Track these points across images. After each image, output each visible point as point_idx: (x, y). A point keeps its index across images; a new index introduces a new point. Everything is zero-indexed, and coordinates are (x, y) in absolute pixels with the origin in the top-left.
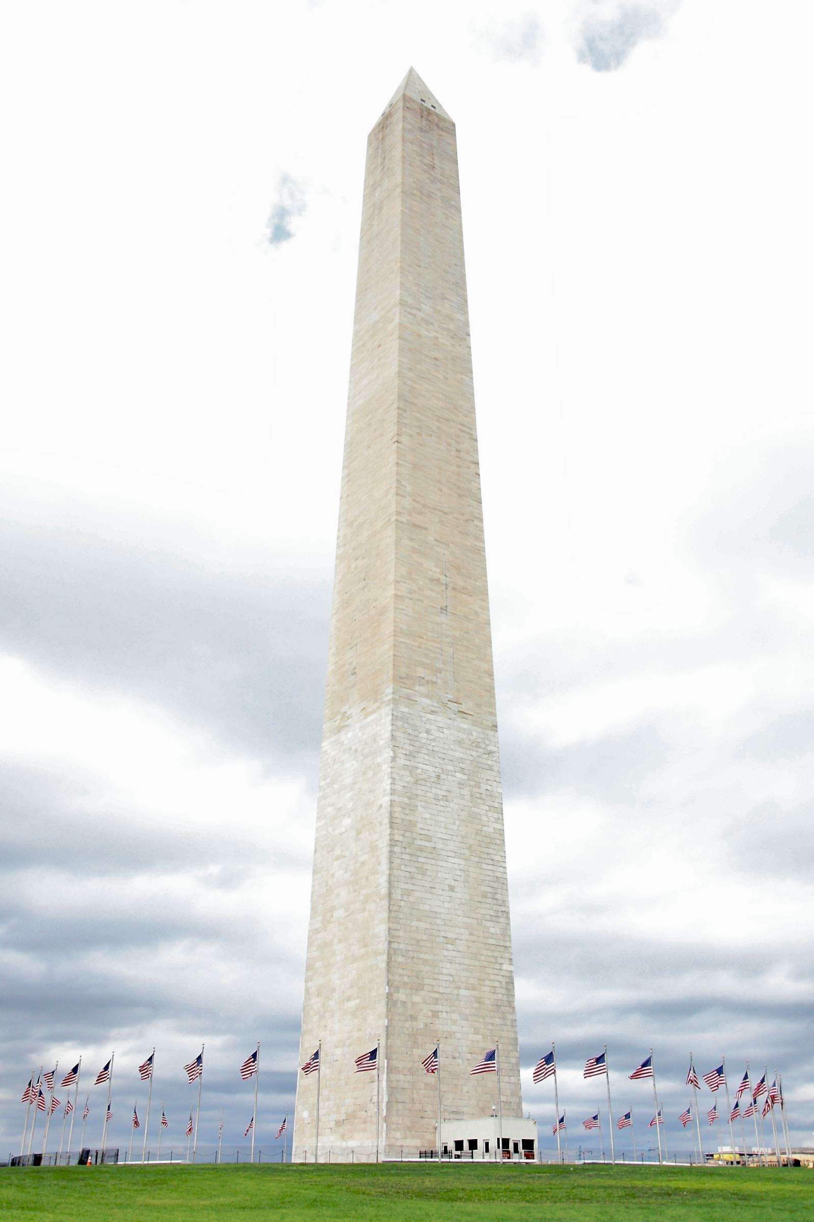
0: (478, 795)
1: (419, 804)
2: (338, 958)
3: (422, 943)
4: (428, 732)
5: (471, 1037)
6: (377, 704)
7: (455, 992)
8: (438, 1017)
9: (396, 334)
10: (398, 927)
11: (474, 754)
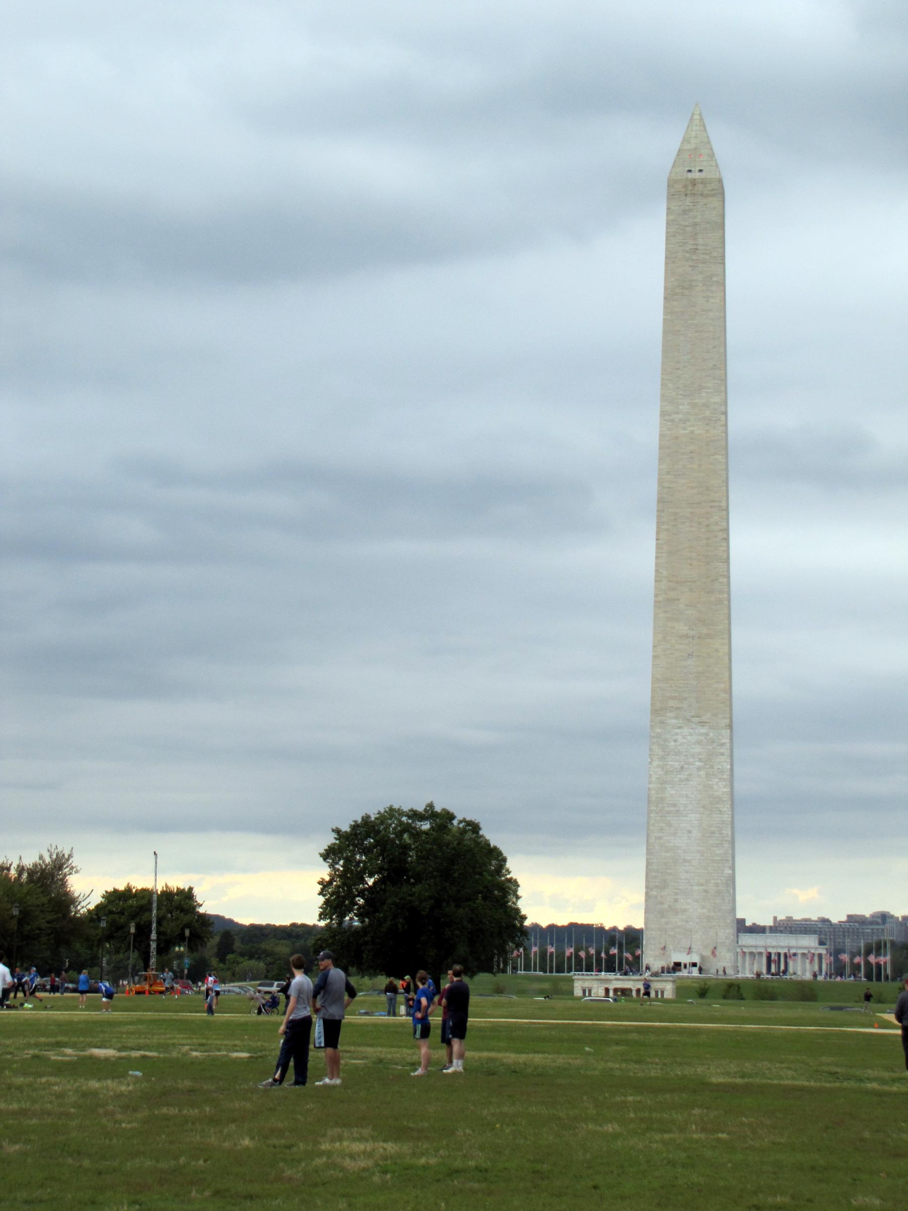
4: (675, 741)
5: (699, 910)
11: (710, 747)
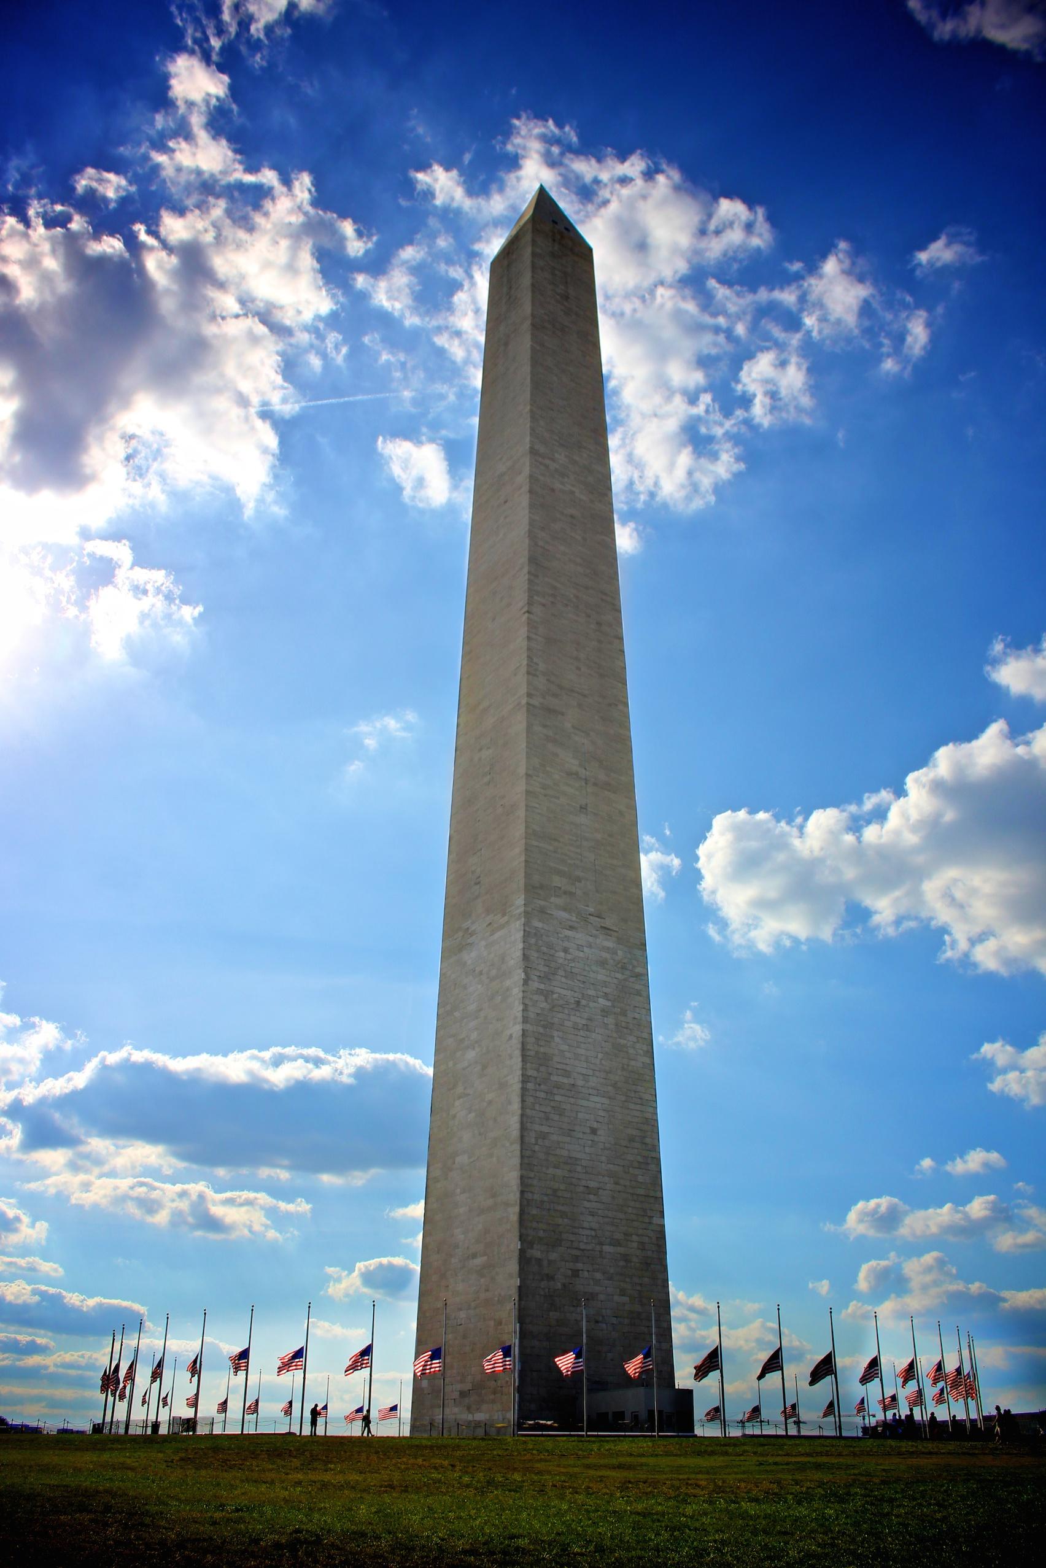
0: (623, 1024)
1: (555, 1034)
2: (462, 1210)
3: (560, 1193)
5: (616, 1298)
6: (506, 918)
7: (598, 1248)
8: (578, 1276)
9: (526, 488)
10: (532, 1175)
11: (619, 976)
